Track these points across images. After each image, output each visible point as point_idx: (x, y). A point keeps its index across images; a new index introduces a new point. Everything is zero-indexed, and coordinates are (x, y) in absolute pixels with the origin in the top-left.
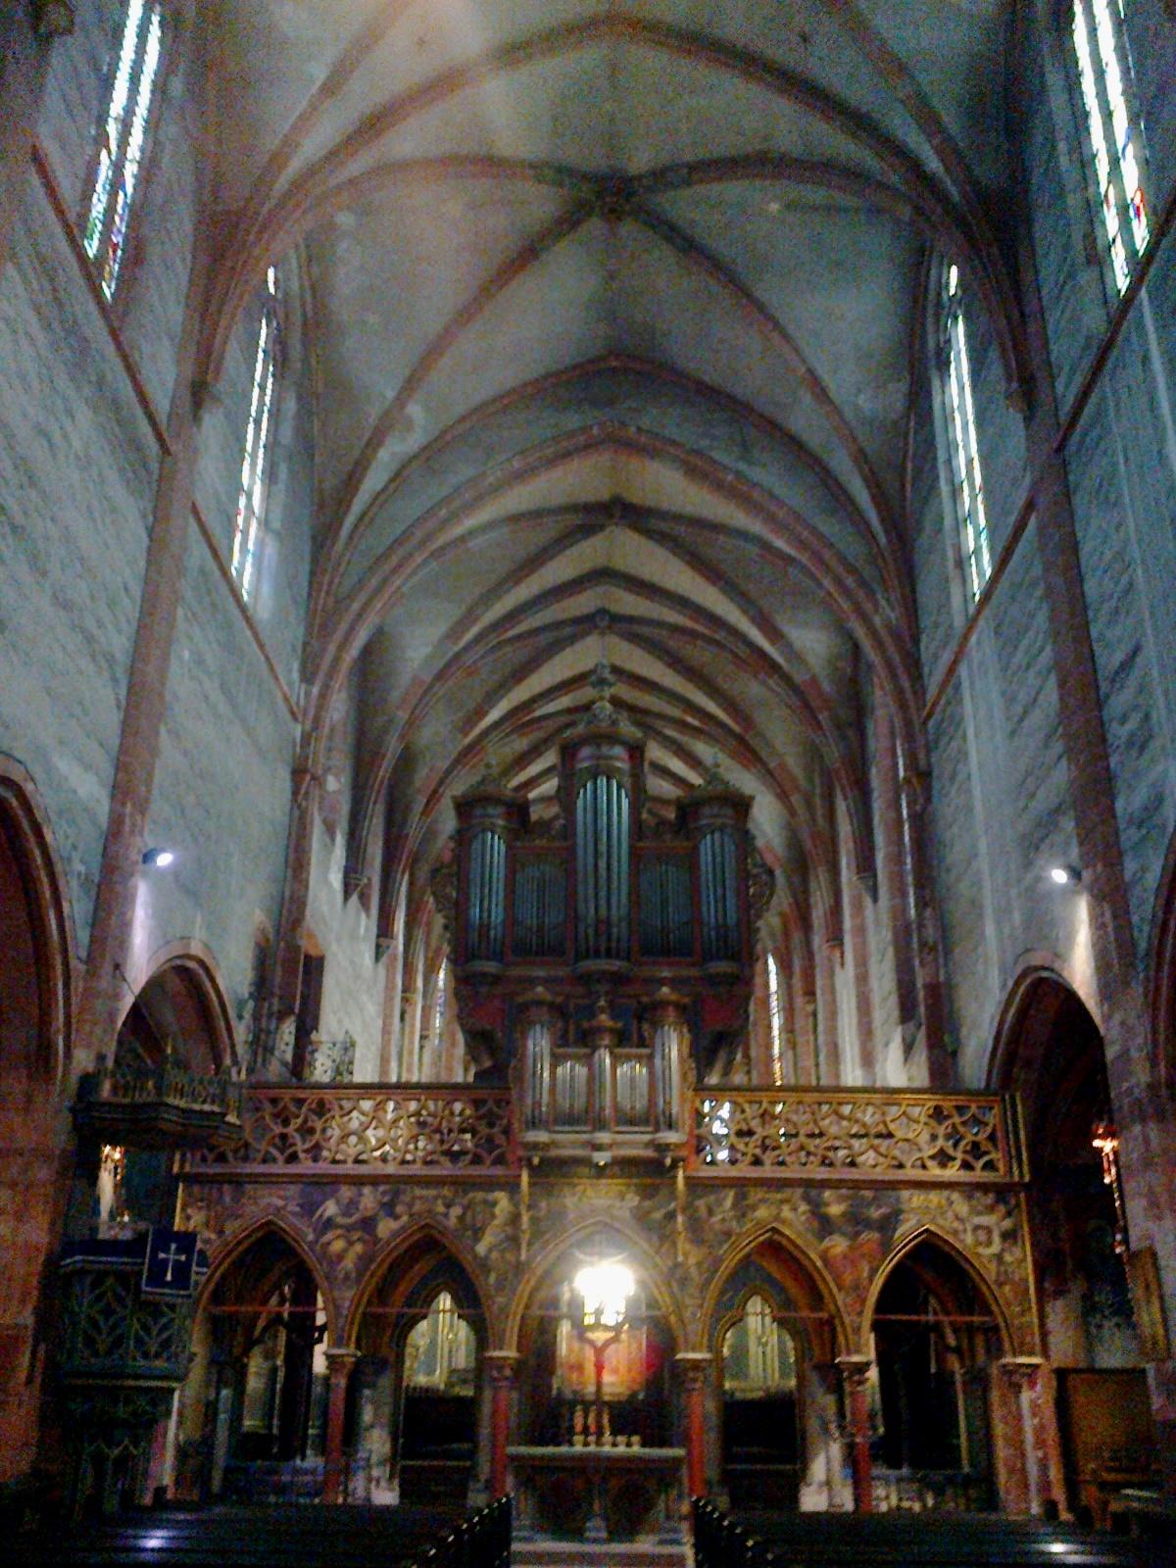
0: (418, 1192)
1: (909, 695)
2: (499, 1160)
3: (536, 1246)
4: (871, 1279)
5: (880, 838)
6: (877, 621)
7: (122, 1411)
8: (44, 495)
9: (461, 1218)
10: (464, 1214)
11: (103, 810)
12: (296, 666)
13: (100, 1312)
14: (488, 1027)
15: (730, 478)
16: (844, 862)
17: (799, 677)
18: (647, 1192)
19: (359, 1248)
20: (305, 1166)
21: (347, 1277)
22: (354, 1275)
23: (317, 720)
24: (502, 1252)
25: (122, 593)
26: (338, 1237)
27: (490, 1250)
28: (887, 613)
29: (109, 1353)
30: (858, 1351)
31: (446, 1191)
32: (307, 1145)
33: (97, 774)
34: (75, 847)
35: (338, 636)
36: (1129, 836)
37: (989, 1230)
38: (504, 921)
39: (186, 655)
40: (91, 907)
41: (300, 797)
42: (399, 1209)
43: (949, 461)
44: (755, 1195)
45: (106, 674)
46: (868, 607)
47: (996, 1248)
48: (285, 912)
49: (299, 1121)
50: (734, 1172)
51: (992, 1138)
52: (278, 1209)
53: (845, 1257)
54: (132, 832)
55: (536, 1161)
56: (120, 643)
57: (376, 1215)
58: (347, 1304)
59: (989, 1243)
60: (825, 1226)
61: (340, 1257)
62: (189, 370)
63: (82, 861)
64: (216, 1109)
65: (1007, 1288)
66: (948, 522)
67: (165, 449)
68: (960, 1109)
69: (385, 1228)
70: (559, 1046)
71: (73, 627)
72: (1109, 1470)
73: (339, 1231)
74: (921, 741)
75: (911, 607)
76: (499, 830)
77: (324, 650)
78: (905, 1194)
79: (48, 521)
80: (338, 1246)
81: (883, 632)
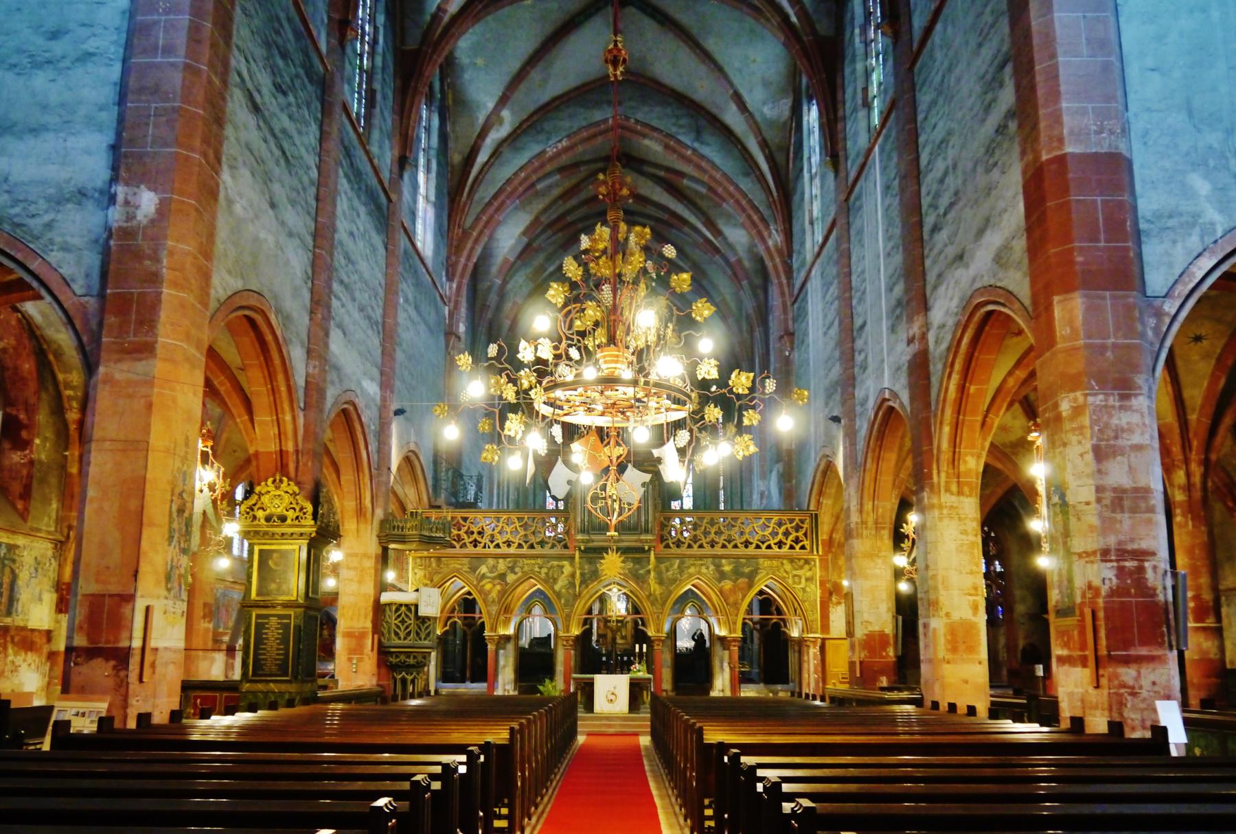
0: (526, 561)
1: (786, 289)
2: (566, 547)
3: (583, 586)
4: (743, 599)
5: (772, 358)
6: (770, 243)
7: (412, 661)
9: (547, 574)
11: (378, 398)
12: (444, 274)
15: (689, 152)
16: (757, 360)
17: (733, 259)
18: (637, 561)
19: (498, 587)
20: (470, 549)
21: (493, 601)
24: (567, 589)
27: (562, 587)
28: (775, 238)
29: (405, 639)
30: (735, 632)
31: (539, 561)
32: (471, 540)
35: (465, 253)
36: (858, 409)
37: (800, 577)
39: (401, 300)
42: (517, 569)
43: (809, 158)
44: (688, 562)
46: (766, 234)
47: (803, 585)
49: (466, 528)
50: (679, 551)
51: (805, 534)
52: (458, 571)
53: (731, 590)
55: (582, 548)
56: (378, 314)
59: (800, 583)
60: (722, 576)
61: (490, 592)
62: (396, 153)
65: (806, 604)
66: (807, 196)
67: (389, 200)
68: (791, 521)
69: (511, 578)
72: (841, 682)
74: (790, 316)
75: (788, 234)
77: (457, 262)
78: (761, 561)
80: (488, 586)
81: (773, 249)
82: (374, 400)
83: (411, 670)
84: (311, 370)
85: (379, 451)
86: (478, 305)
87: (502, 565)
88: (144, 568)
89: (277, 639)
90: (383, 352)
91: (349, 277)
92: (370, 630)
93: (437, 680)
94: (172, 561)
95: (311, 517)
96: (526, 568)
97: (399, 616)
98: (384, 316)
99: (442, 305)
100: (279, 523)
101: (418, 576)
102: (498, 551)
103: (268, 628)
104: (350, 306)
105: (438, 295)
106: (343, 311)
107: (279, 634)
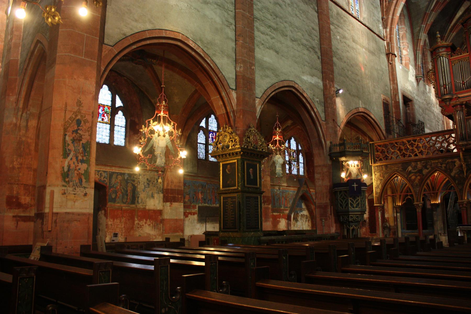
7: (350, 220)
8: (281, 18)
10: (446, 166)
13: (342, 199)
14: (451, 114)
19: (419, 177)
21: (417, 185)
22: (418, 184)
23: (390, 38)
25: (313, 30)
26: (414, 175)
27: (455, 174)
31: (440, 160)
32: (401, 154)
33: (316, 76)
34: (314, 95)
38: (451, 82)
40: (323, 108)
41: (390, 62)
42: (428, 167)
45: (313, 52)
48: (392, 93)
54: (330, 87)
57: (422, 168)
58: (418, 192)
61: (414, 180)
63: (317, 98)
64: (359, 150)
69: (425, 172)
70: (466, 116)
71: (299, 45)
73: (413, 174)
76: (444, 56)
77: (388, 18)
79: (284, 23)
80: (413, 177)
82: (318, 87)
83: (351, 224)
84: (238, 69)
85: (325, 111)
86: (416, 41)
87: (419, 165)
88: (50, 171)
89: (231, 209)
90: (322, 63)
91: (277, 24)
92: (329, 204)
93: (402, 229)
94: (69, 166)
95: (238, 144)
96: (433, 165)
97: (341, 196)
98: (321, 44)
99: (381, 40)
100: (227, 149)
101: (377, 176)
102: (417, 158)
103: (227, 204)
104: (282, 39)
105: (376, 35)
106: (273, 40)
107: (232, 207)
